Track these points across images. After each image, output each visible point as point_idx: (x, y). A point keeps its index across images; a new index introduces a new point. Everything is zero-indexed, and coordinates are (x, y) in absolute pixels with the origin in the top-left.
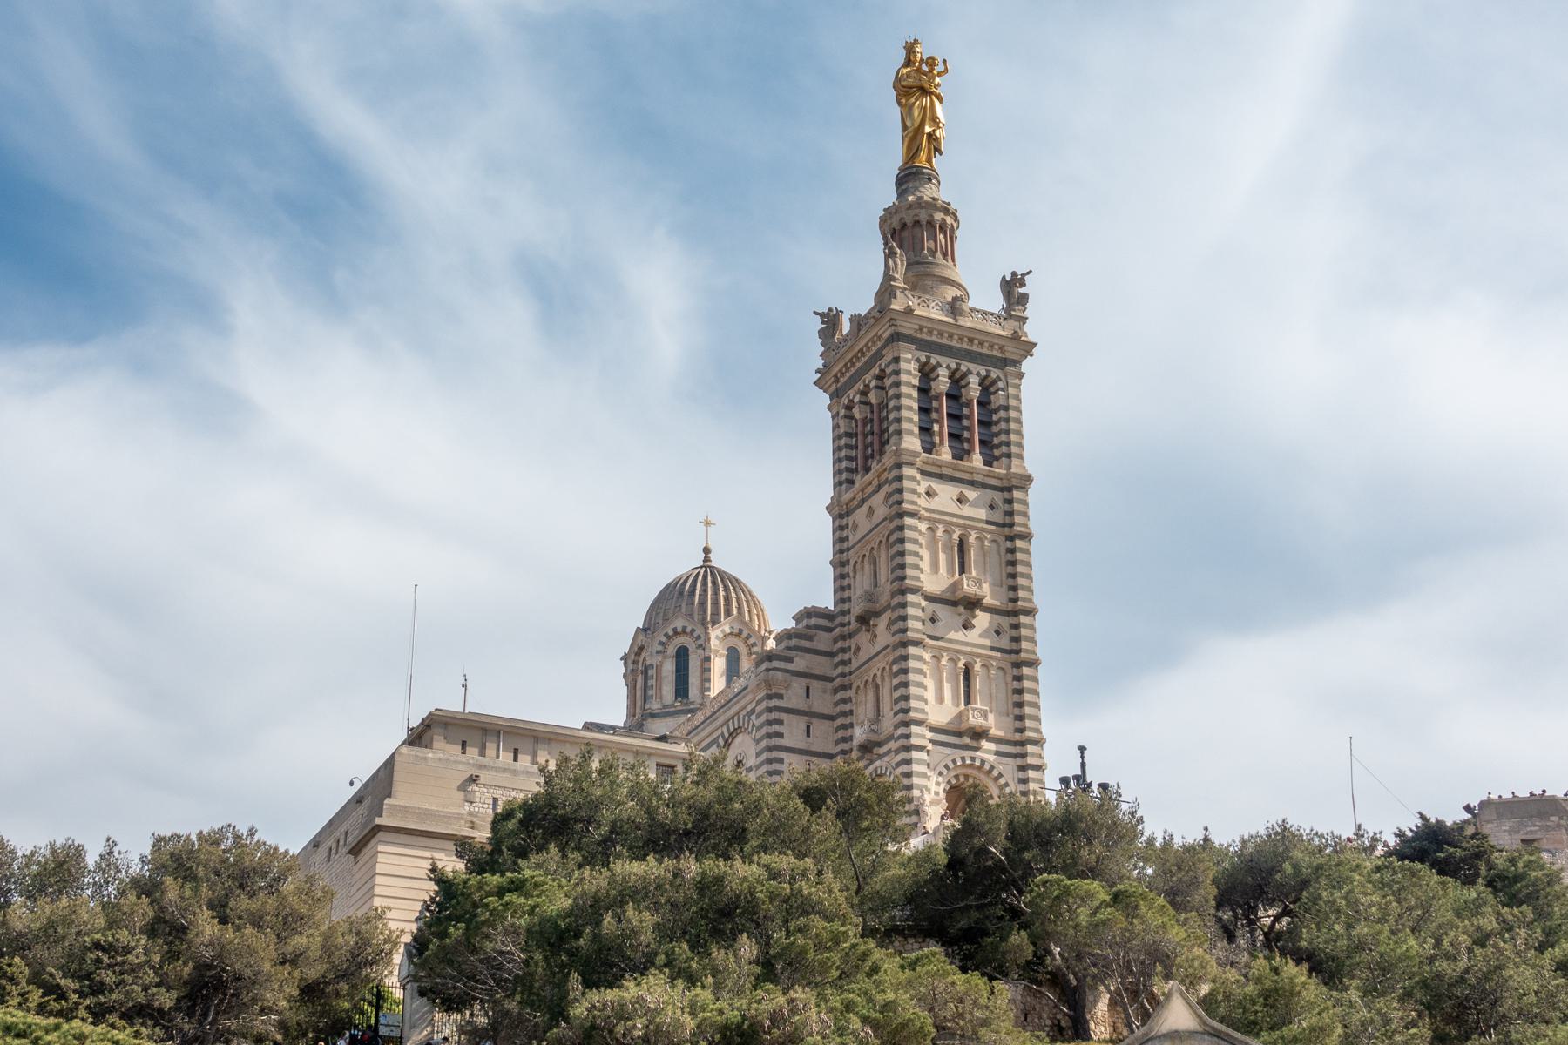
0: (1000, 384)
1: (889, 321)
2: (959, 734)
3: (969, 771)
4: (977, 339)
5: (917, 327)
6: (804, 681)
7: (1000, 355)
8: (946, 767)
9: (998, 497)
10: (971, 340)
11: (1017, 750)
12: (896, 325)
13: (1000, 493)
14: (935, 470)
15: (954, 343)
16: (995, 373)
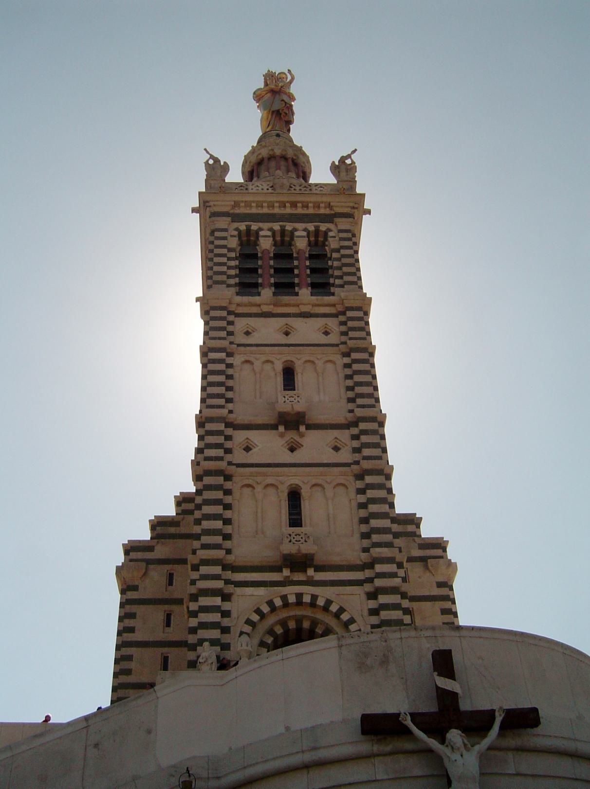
0: (331, 234)
1: (204, 206)
2: (278, 569)
3: (299, 612)
4: (298, 202)
5: (233, 203)
6: (167, 568)
7: (327, 211)
8: (258, 611)
9: (332, 324)
10: (294, 205)
11: (368, 573)
12: (210, 206)
13: (336, 319)
14: (255, 310)
15: (277, 211)
16: (323, 227)
